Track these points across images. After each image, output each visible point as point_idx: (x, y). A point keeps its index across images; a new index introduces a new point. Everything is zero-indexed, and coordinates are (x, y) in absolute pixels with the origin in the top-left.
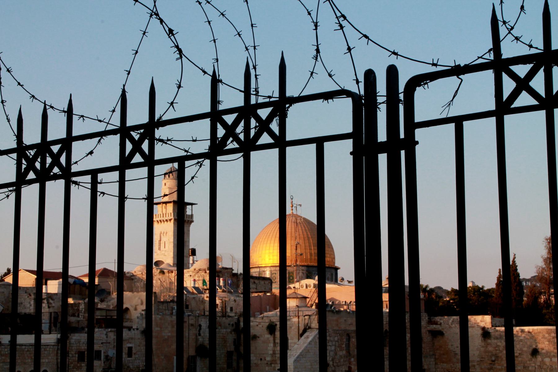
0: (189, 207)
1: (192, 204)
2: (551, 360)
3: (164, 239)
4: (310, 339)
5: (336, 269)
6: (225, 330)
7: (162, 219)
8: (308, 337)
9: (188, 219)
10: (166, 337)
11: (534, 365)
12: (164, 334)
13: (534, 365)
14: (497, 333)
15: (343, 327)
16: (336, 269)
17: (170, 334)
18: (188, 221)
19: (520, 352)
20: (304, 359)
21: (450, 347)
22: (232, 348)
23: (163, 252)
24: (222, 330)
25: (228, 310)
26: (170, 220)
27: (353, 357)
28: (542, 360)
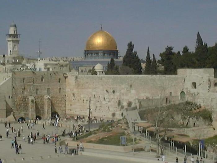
1: (19, 35)
3: (10, 46)
25: (7, 70)
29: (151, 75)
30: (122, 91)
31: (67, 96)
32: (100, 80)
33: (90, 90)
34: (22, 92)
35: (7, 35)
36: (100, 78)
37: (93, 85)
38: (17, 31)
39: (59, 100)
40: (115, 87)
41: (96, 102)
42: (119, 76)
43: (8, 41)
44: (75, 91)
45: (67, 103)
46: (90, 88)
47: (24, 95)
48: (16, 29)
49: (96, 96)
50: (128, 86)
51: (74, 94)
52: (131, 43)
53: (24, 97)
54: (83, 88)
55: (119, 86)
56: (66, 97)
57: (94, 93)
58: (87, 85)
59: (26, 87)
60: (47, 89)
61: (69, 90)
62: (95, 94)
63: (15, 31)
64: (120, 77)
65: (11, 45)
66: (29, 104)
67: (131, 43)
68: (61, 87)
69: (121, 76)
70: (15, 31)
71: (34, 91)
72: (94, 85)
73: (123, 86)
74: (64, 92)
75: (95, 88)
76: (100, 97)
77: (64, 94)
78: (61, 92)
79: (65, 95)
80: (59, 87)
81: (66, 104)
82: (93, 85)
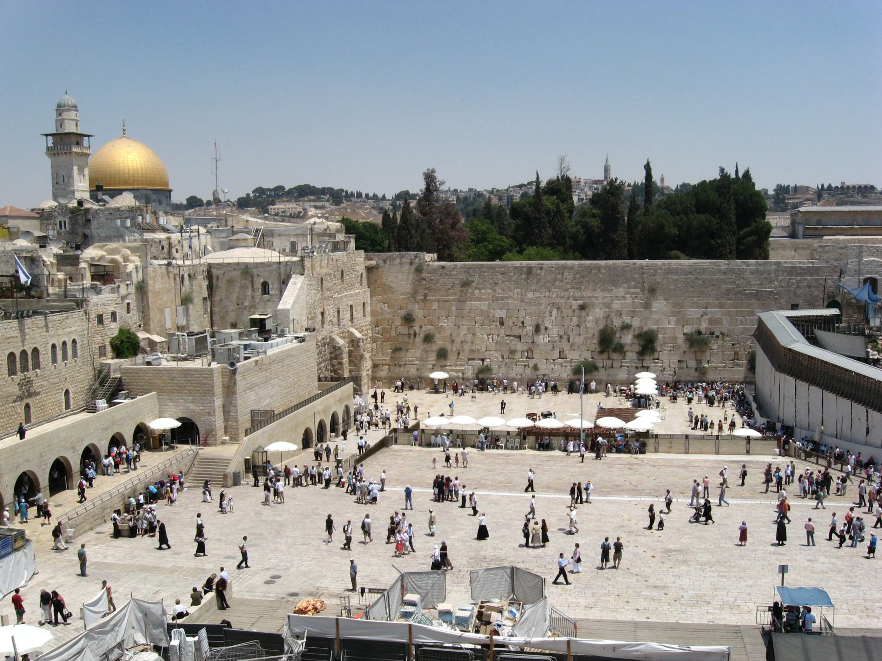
0: (86, 138)
1: (89, 136)
4: (299, 285)
5: (170, 191)
8: (295, 283)
16: (170, 191)
25: (174, 250)
29: (726, 261)
30: (616, 305)
33: (483, 305)
35: (47, 135)
40: (587, 293)
42: (602, 263)
46: (480, 300)
49: (509, 323)
50: (638, 290)
52: (433, 171)
55: (603, 290)
57: (502, 313)
62: (504, 316)
64: (608, 268)
67: (433, 171)
69: (611, 262)
72: (500, 291)
73: (620, 292)
75: (495, 299)
76: (523, 323)
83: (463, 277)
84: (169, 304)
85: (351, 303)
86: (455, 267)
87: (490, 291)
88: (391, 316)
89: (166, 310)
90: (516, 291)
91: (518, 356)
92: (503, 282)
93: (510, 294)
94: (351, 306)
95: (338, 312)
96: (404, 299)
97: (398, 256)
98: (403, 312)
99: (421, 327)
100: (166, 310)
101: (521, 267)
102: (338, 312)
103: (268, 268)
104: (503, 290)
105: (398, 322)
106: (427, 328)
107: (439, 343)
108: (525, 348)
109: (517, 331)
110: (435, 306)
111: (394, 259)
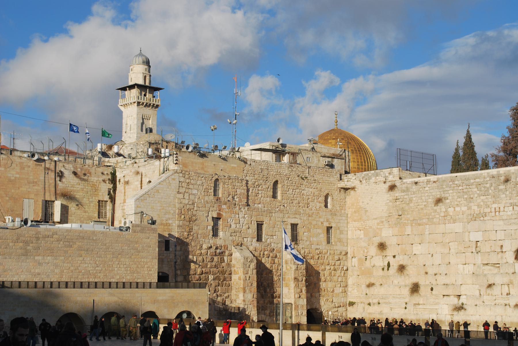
2: (455, 210)
6: (96, 179)
7: (127, 102)
9: (154, 103)
10: (13, 178)
11: (438, 216)
12: (10, 175)
13: (438, 216)
14: (404, 186)
15: (211, 171)
17: (18, 176)
18: (154, 104)
19: (426, 203)
20: (151, 199)
21: (361, 204)
22: (106, 198)
23: (129, 135)
24: (92, 178)
26: (135, 103)
27: (225, 204)
28: (446, 211)
31: (349, 255)
32: (502, 187)
33: (458, 227)
34: (210, 228)
36: (502, 178)
37: (469, 208)
38: (150, 76)
39: (328, 267)
41: (487, 267)
43: (125, 105)
44: (387, 234)
45: (350, 282)
47: (219, 242)
48: (149, 72)
49: (485, 247)
51: (382, 246)
53: (217, 248)
54: (424, 221)
56: (346, 260)
57: (475, 236)
58: (441, 207)
59: (224, 214)
60: (290, 227)
61: (361, 234)
63: (145, 77)
65: (135, 116)
66: (234, 277)
68: (333, 225)
70: (145, 77)
71: (250, 231)
72: (475, 208)
74: (340, 240)
77: (339, 248)
78: (332, 240)
79: (344, 253)
80: (326, 224)
81: (346, 286)
82: (469, 208)
83: (438, 194)
84: (32, 196)
85: (294, 221)
86: (428, 181)
87: (464, 209)
88: (366, 245)
89: (26, 201)
90: (494, 206)
91: (496, 290)
92: (479, 195)
93: (487, 210)
94: (294, 227)
95: (260, 226)
96: (378, 224)
97: (373, 174)
98: (377, 240)
99: (394, 257)
100: (26, 201)
101: (499, 176)
102: (260, 226)
103: (152, 167)
104: (479, 206)
105: (373, 250)
106: (401, 260)
107: (413, 276)
108: (506, 280)
109: (494, 259)
110: (408, 230)
111: (370, 178)
